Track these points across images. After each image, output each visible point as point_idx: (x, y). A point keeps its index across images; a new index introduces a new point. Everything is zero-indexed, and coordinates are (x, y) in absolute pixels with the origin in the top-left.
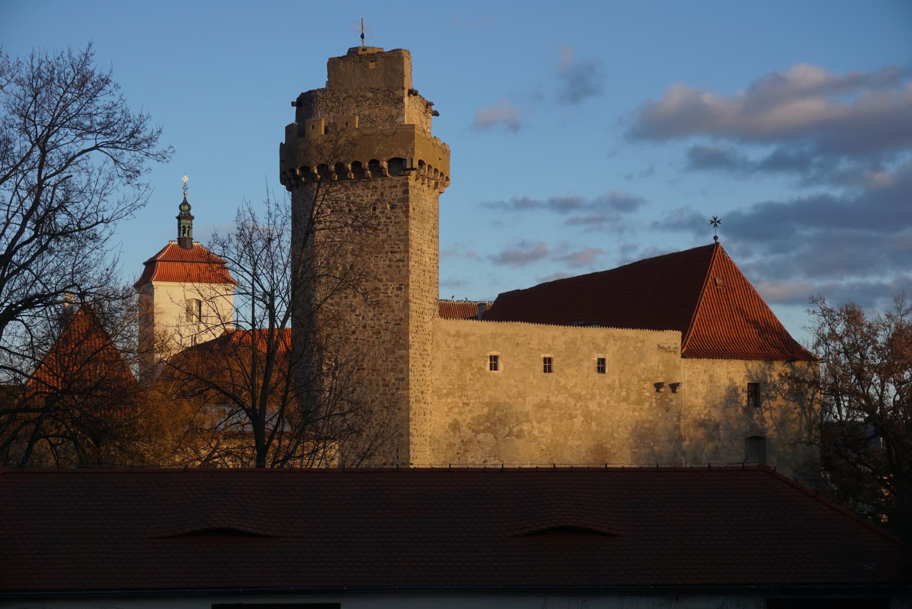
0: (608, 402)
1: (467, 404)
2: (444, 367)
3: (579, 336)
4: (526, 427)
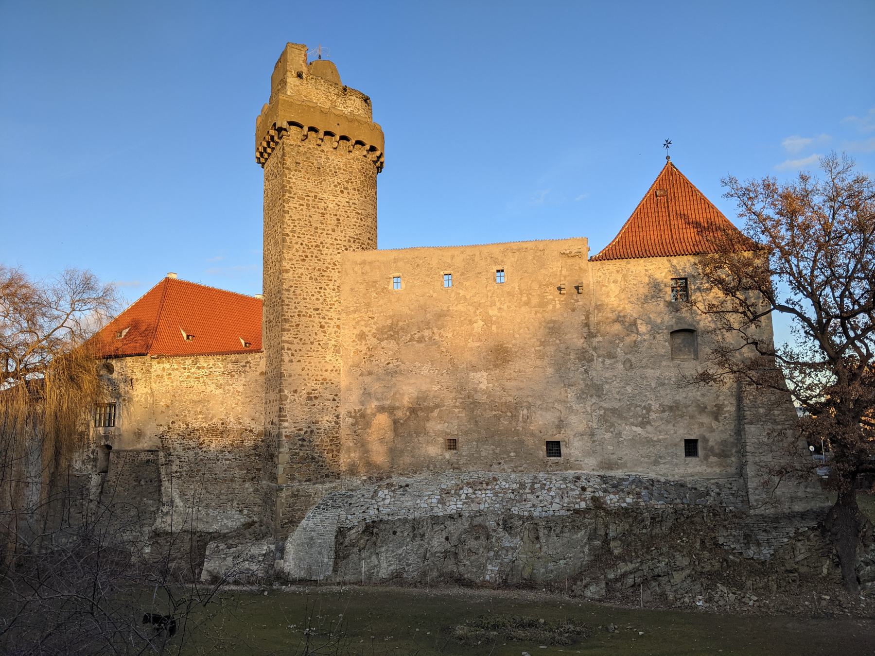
0: (509, 307)
1: (372, 318)
2: (352, 290)
3: (478, 253)
4: (427, 333)
